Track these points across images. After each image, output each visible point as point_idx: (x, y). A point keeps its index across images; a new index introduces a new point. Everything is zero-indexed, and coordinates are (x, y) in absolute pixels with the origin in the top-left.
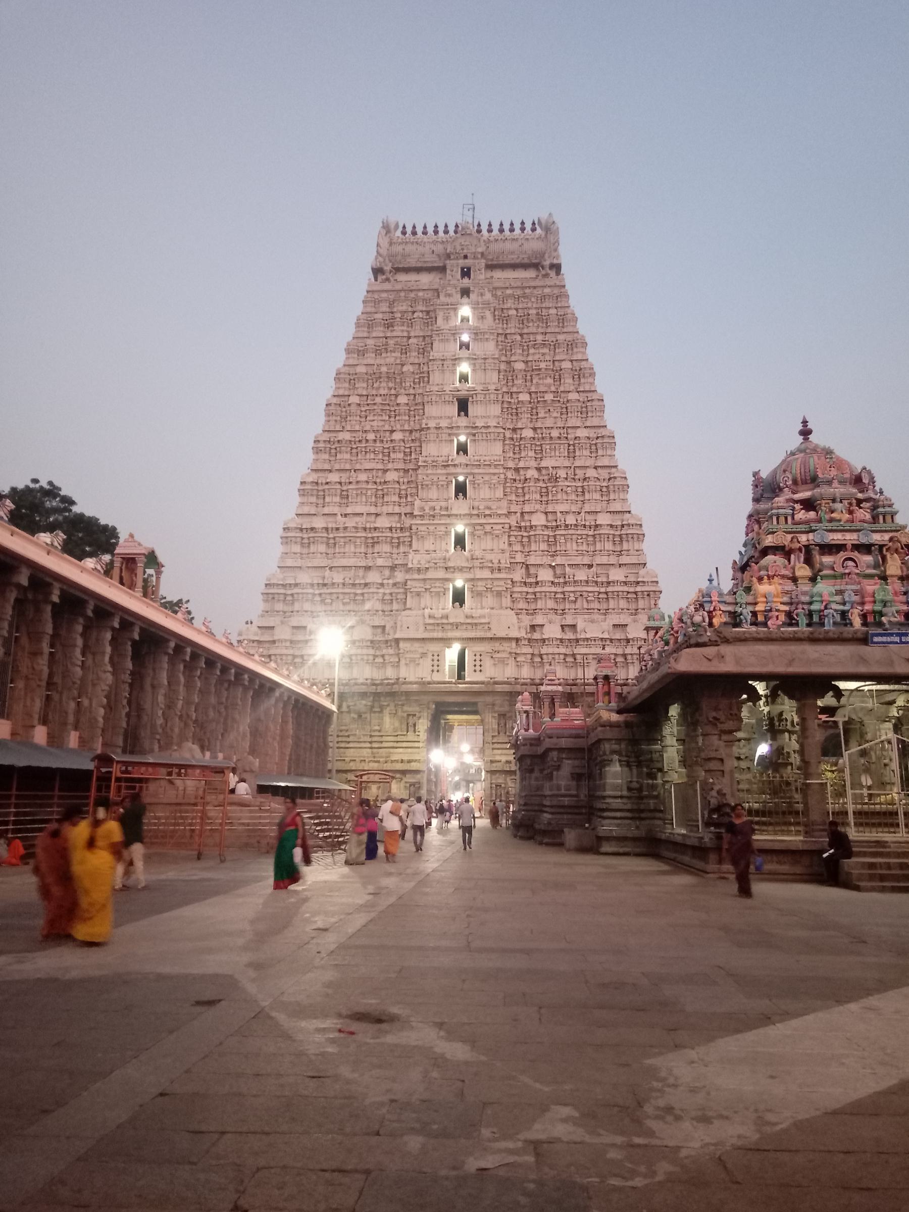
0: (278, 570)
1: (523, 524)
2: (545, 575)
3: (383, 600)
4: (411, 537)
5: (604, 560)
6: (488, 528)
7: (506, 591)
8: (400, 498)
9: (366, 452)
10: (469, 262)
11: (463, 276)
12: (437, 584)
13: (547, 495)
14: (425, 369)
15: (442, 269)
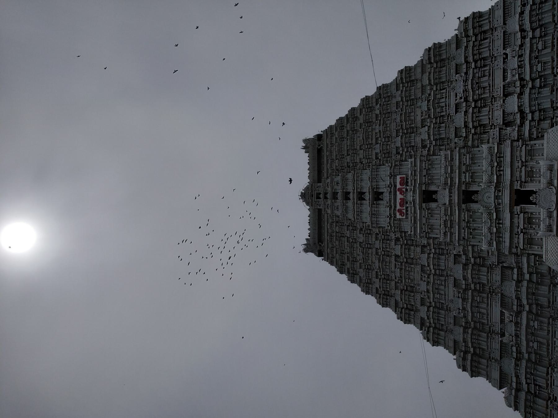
0: (503, 390)
1: (464, 135)
2: (513, 104)
3: (537, 283)
4: (473, 246)
5: (499, 43)
6: (464, 168)
7: (526, 145)
8: (442, 254)
9: (409, 278)
10: (315, 194)
11: (320, 198)
12: (516, 220)
13: (443, 116)
14: (361, 224)
15: (320, 211)
